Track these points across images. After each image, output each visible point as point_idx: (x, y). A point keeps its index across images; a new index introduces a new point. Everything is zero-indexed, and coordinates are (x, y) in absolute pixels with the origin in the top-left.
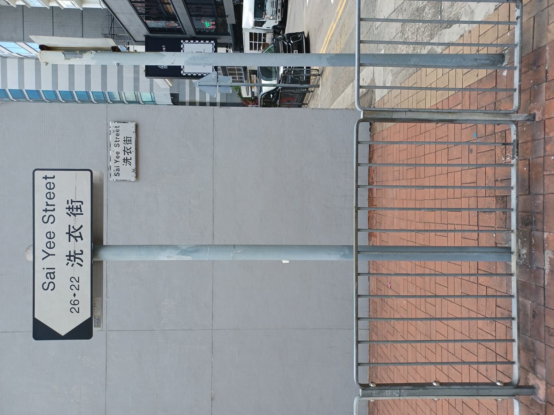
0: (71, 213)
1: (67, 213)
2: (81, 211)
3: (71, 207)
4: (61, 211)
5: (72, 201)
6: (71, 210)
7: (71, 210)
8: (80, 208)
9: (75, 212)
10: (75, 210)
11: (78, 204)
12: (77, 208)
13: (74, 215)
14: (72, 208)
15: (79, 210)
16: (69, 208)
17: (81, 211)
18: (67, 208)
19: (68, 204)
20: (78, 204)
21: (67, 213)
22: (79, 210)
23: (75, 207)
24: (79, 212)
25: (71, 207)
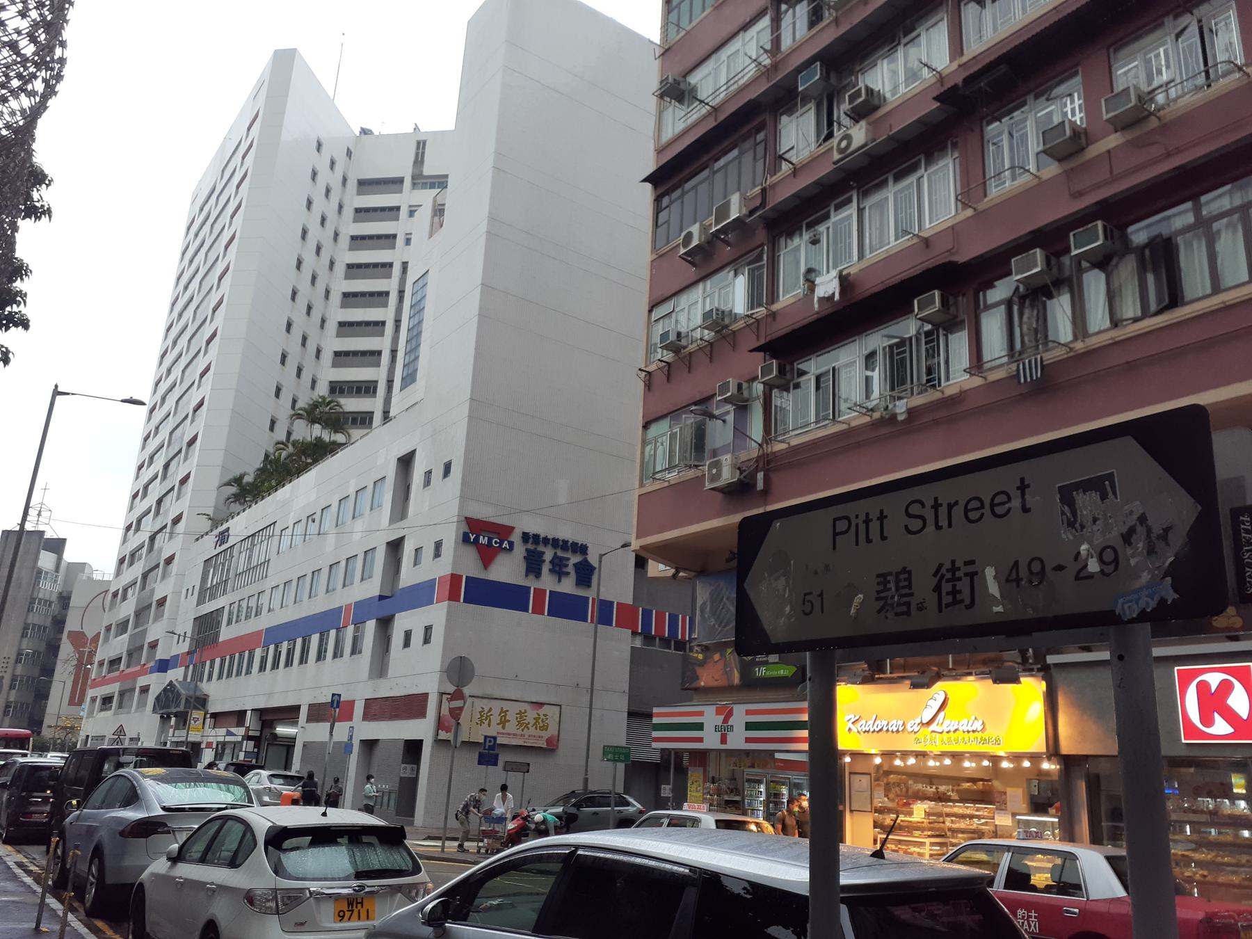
0: (943, 576)
5: (972, 575)
8: (956, 602)
9: (947, 587)
12: (954, 592)
13: (937, 589)
15: (949, 599)
17: (948, 605)
21: (941, 566)
22: (949, 599)
23: (959, 585)
25: (958, 574)
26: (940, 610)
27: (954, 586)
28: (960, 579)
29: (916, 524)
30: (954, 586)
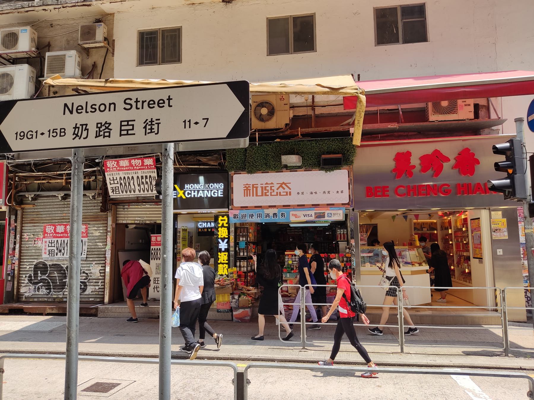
1: (147, 120)
2: (148, 133)
3: (153, 123)
5: (158, 124)
6: (150, 123)
7: (150, 123)
8: (151, 132)
9: (148, 127)
10: (150, 127)
11: (156, 130)
12: (151, 129)
13: (145, 127)
15: (150, 131)
16: (152, 121)
17: (148, 133)
18: (152, 119)
19: (157, 120)
20: (156, 130)
22: (150, 131)
24: (148, 131)
25: (153, 123)
26: (146, 135)
27: (151, 127)
28: (154, 125)
30: (151, 127)
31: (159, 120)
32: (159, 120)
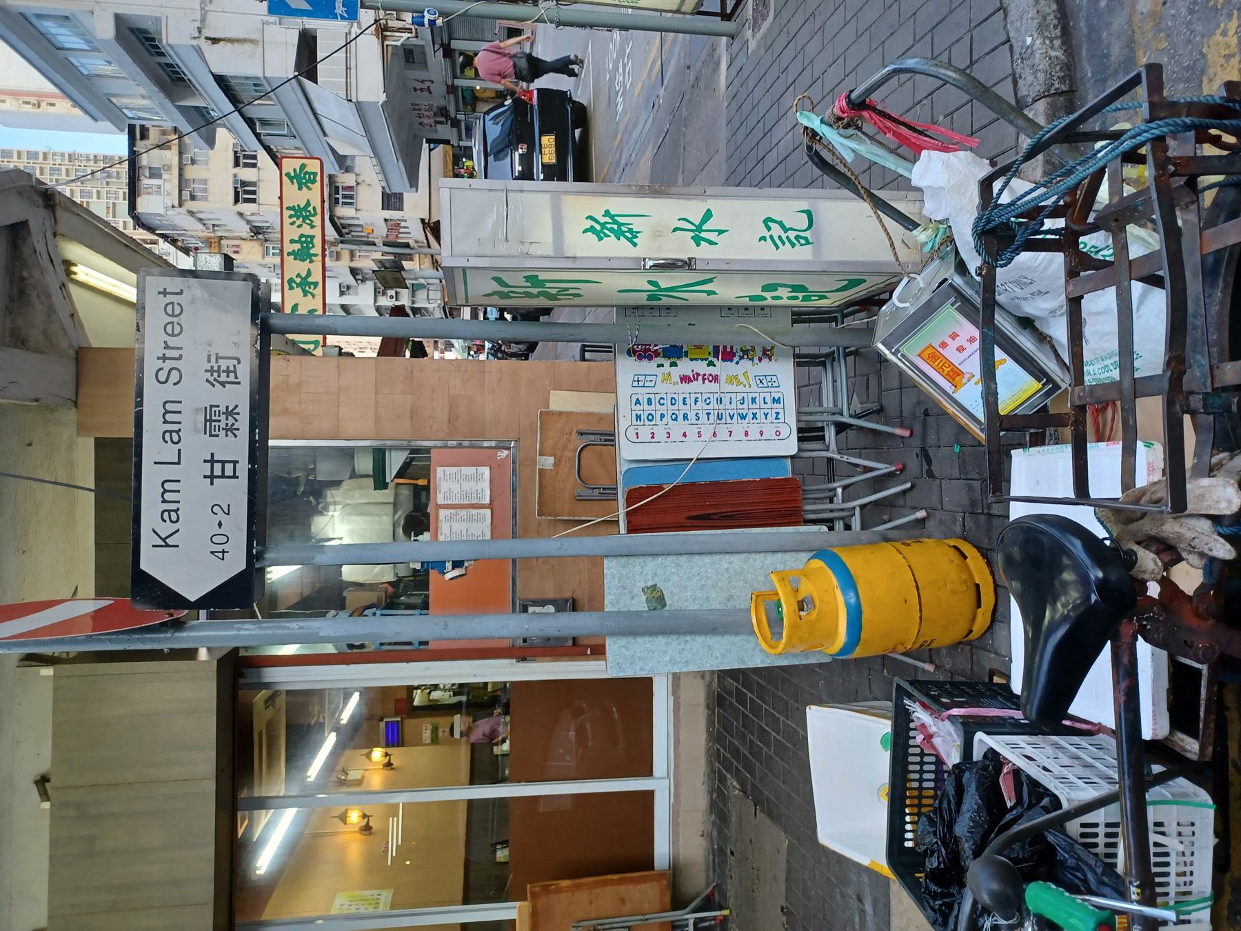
3: (216, 368)
4: (194, 365)
8: (235, 372)
9: (223, 377)
12: (228, 372)
14: (218, 371)
15: (232, 375)
19: (209, 361)
22: (232, 375)
23: (223, 368)
24: (232, 378)
25: (216, 368)
29: (175, 376)
31: (209, 356)
32: (209, 356)
